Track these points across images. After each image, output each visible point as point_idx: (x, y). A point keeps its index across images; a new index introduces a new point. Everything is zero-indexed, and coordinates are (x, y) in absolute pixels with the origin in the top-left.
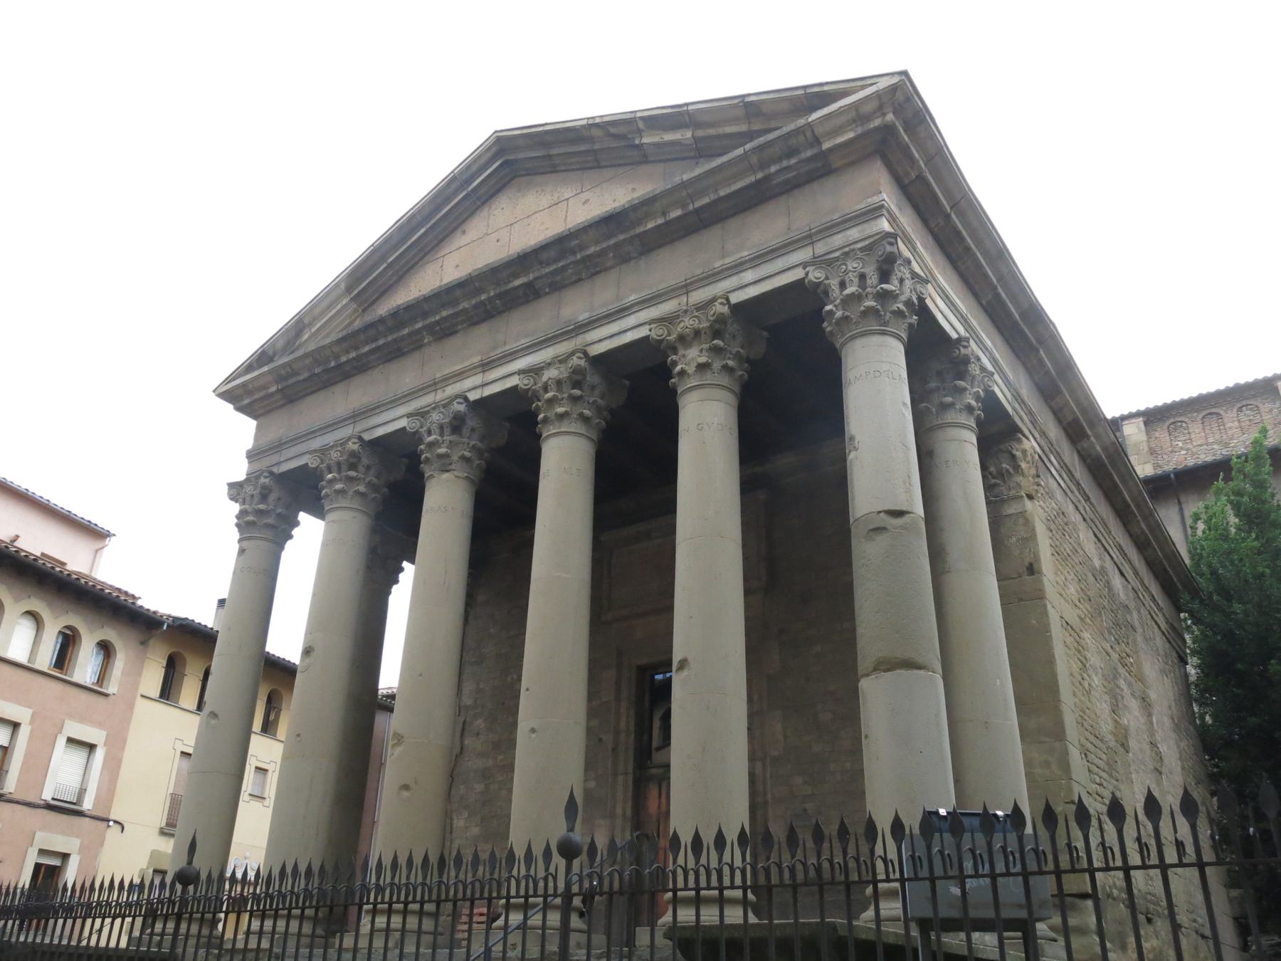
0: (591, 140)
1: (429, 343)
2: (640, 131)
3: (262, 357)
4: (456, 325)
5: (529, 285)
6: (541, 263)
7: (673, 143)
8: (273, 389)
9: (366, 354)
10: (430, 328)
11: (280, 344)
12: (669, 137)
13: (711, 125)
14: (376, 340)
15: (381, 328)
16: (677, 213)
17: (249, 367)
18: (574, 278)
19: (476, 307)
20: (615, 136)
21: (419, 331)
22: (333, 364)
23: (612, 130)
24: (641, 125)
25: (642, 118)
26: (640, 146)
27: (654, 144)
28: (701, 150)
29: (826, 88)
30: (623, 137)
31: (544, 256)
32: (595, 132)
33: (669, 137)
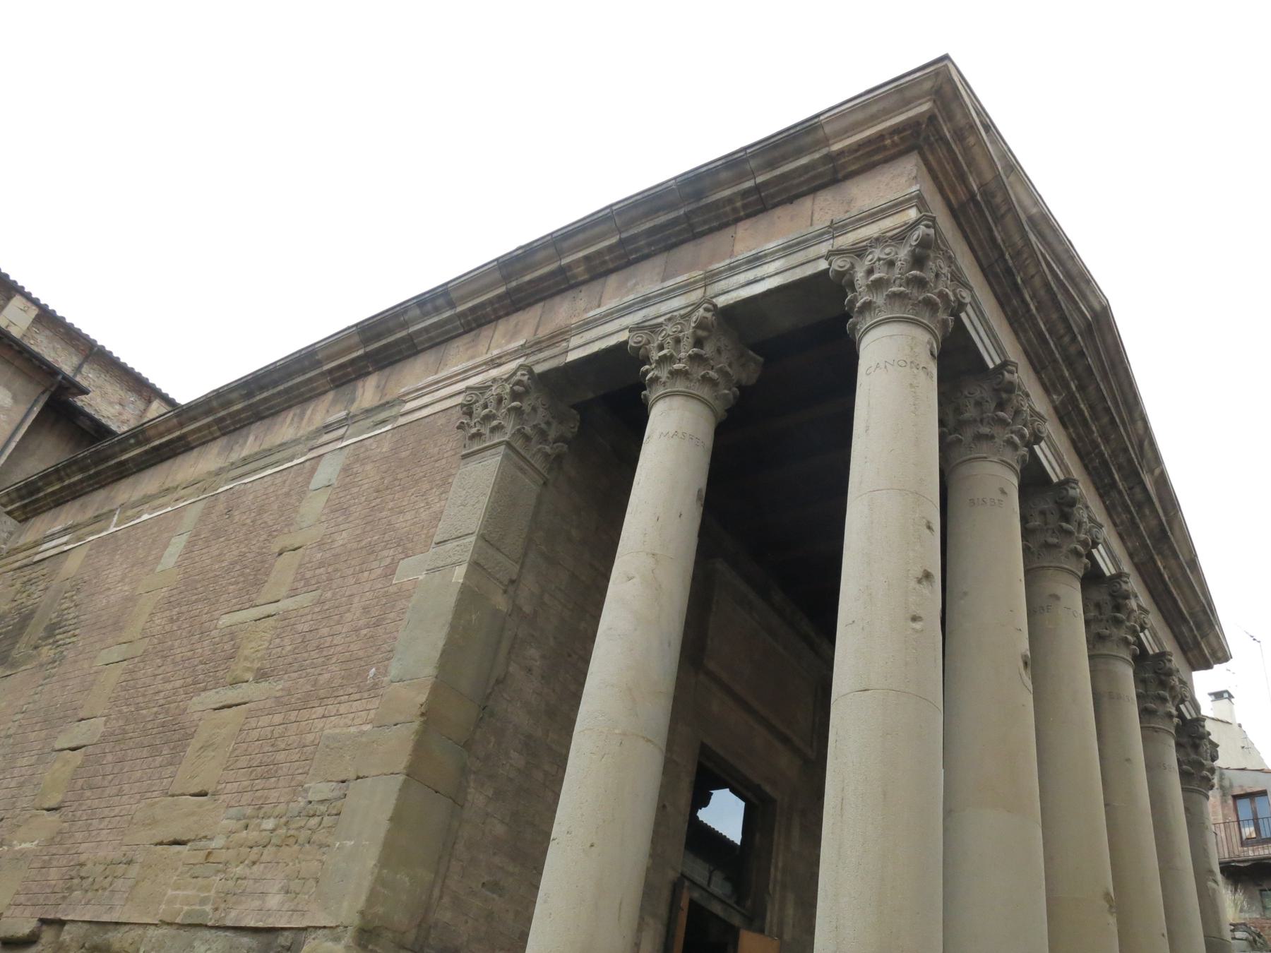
0: (1133, 421)
1: (1052, 401)
2: (1151, 471)
4: (1074, 426)
5: (1114, 484)
6: (1131, 489)
9: (1036, 325)
10: (1072, 399)
15: (1067, 339)
17: (982, 112)
18: (1118, 521)
19: (1093, 442)
20: (1141, 446)
21: (1068, 387)
23: (1146, 443)
24: (1157, 472)
31: (1137, 490)
32: (1140, 424)
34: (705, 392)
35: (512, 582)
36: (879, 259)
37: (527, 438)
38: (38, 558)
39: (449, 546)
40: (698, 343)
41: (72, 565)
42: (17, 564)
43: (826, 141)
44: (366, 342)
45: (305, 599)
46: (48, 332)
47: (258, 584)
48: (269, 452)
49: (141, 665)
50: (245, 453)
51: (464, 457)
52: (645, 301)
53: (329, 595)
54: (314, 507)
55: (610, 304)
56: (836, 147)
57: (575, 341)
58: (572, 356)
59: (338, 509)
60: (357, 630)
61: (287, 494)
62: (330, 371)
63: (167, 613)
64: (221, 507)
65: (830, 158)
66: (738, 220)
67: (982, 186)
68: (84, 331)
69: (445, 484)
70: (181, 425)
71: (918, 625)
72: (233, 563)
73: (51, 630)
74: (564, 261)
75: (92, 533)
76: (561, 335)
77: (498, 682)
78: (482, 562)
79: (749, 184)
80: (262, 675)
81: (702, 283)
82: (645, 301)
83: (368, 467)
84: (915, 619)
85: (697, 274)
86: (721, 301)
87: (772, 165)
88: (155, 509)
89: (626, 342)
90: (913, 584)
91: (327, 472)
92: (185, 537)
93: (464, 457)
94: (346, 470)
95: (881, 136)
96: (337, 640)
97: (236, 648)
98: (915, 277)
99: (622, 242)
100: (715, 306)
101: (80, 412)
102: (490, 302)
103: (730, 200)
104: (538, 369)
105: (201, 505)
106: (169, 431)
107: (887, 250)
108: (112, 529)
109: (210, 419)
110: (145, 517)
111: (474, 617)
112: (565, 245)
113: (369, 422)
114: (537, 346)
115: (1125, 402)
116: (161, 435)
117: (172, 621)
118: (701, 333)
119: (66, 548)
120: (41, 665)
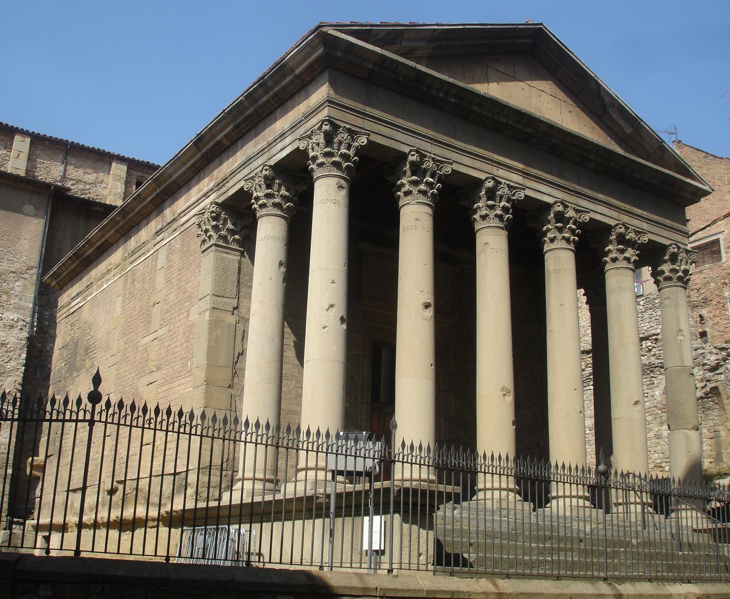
3: (365, 33)
8: (370, 66)
22: (425, 88)
23: (603, 95)
27: (614, 120)
29: (691, 170)
35: (235, 308)
36: (314, 143)
38: (72, 311)
39: (203, 301)
40: (269, 186)
41: (85, 313)
42: (65, 315)
43: (293, 70)
44: (159, 186)
45: (165, 330)
46: (40, 147)
47: (149, 322)
48: (140, 248)
49: (120, 366)
50: (132, 248)
51: (203, 252)
53: (172, 327)
54: (160, 278)
56: (297, 72)
59: (168, 281)
61: (151, 272)
62: (150, 201)
63: (123, 340)
64: (130, 280)
65: (298, 77)
66: (276, 109)
68: (59, 138)
70: (103, 236)
71: (326, 330)
72: (140, 311)
73: (87, 350)
74: (218, 139)
75: (88, 296)
76: (225, 180)
77: (239, 355)
78: (216, 306)
79: (271, 94)
80: (158, 368)
83: (175, 256)
84: (324, 328)
86: (272, 162)
87: (277, 83)
88: (108, 281)
90: (324, 312)
91: (161, 261)
92: (120, 298)
93: (203, 252)
94: (167, 258)
95: (311, 65)
96: (177, 349)
97: (148, 355)
98: (325, 152)
99: (236, 127)
100: (270, 166)
102: (198, 161)
103: (268, 102)
104: (220, 201)
106: (101, 239)
107: (316, 138)
109: (112, 231)
110: (105, 286)
111: (219, 332)
112: (214, 131)
113: (170, 230)
114: (219, 185)
116: (98, 241)
117: (126, 343)
118: (268, 182)
119: (81, 305)
120: (88, 370)
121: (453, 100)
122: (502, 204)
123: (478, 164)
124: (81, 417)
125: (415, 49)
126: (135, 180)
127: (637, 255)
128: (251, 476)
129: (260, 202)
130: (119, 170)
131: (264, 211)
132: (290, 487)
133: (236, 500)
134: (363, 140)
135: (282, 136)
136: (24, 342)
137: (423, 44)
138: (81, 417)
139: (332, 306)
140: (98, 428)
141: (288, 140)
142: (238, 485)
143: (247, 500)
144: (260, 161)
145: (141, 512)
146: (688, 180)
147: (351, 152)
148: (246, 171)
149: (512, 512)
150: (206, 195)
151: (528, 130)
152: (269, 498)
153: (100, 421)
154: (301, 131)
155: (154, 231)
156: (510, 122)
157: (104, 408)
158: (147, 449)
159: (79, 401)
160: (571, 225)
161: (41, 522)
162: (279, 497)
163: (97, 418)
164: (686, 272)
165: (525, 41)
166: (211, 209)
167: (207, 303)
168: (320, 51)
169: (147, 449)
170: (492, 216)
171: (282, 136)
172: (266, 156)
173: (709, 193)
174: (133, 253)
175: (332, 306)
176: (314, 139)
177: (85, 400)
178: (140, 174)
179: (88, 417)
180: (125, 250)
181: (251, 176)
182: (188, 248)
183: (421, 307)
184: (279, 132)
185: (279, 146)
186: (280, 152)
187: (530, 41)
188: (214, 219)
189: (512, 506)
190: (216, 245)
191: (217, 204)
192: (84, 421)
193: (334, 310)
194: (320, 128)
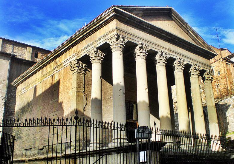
5: (176, 42)
7: (192, 36)
8: (127, 18)
11: (130, 10)
12: (193, 35)
13: (198, 39)
14: (152, 28)
16: (195, 49)
20: (187, 27)
24: (191, 30)
25: (192, 30)
26: (188, 31)
28: (194, 40)
30: (188, 29)
32: (185, 24)
33: (193, 35)
34: (99, 61)
37: (80, 69)
42: (19, 95)
48: (48, 73)
50: (45, 73)
52: (88, 46)
55: (85, 46)
57: (82, 53)
58: (82, 56)
60: (66, 102)
67: (128, 18)
69: (71, 78)
71: (120, 96)
76: (79, 52)
81: (94, 43)
82: (88, 46)
84: (119, 96)
85: (94, 41)
86: (97, 47)
89: (87, 54)
100: (96, 48)
101: (17, 58)
104: (78, 58)
105: (42, 83)
106: (33, 70)
108: (31, 88)
114: (77, 54)
115: (181, 22)
116: (32, 71)
121: (150, 29)
122: (164, 59)
123: (157, 47)
124: (72, 124)
125: (138, 14)
126: (34, 53)
127: (199, 73)
128: (96, 142)
129: (93, 59)
130: (29, 50)
131: (94, 61)
132: (110, 145)
133: (91, 150)
134: (126, 40)
135: (100, 39)
136: (3, 104)
137: (141, 12)
138: (72, 124)
139: (121, 89)
140: (78, 127)
141: (102, 40)
142: (91, 145)
143: (95, 149)
144: (92, 46)
145: (54, 155)
146: (211, 52)
147: (123, 44)
148: (87, 49)
149: (173, 149)
150: (73, 57)
151: (170, 37)
152: (101, 149)
153: (78, 125)
154: (107, 37)
155: (53, 68)
156: (165, 35)
157: (79, 121)
158: (55, 136)
159: (71, 119)
160: (182, 65)
161: (14, 160)
162: (107, 148)
163: (77, 124)
164: (212, 78)
165: (167, 12)
166: (75, 61)
167: (75, 90)
168: (114, 13)
169: (55, 136)
170: (161, 62)
171: (100, 39)
172: (94, 45)
173: (217, 55)
174: (45, 75)
175: (121, 89)
176: (112, 40)
177: (73, 118)
178: (36, 51)
179: (75, 124)
180: (42, 73)
181: (89, 51)
182: (66, 73)
183: (145, 89)
184: (98, 38)
185: (99, 42)
186: (100, 44)
187: (168, 12)
188: (77, 64)
189: (172, 147)
190: (77, 72)
191: (77, 59)
192: (73, 125)
193: (121, 91)
194: (114, 36)
